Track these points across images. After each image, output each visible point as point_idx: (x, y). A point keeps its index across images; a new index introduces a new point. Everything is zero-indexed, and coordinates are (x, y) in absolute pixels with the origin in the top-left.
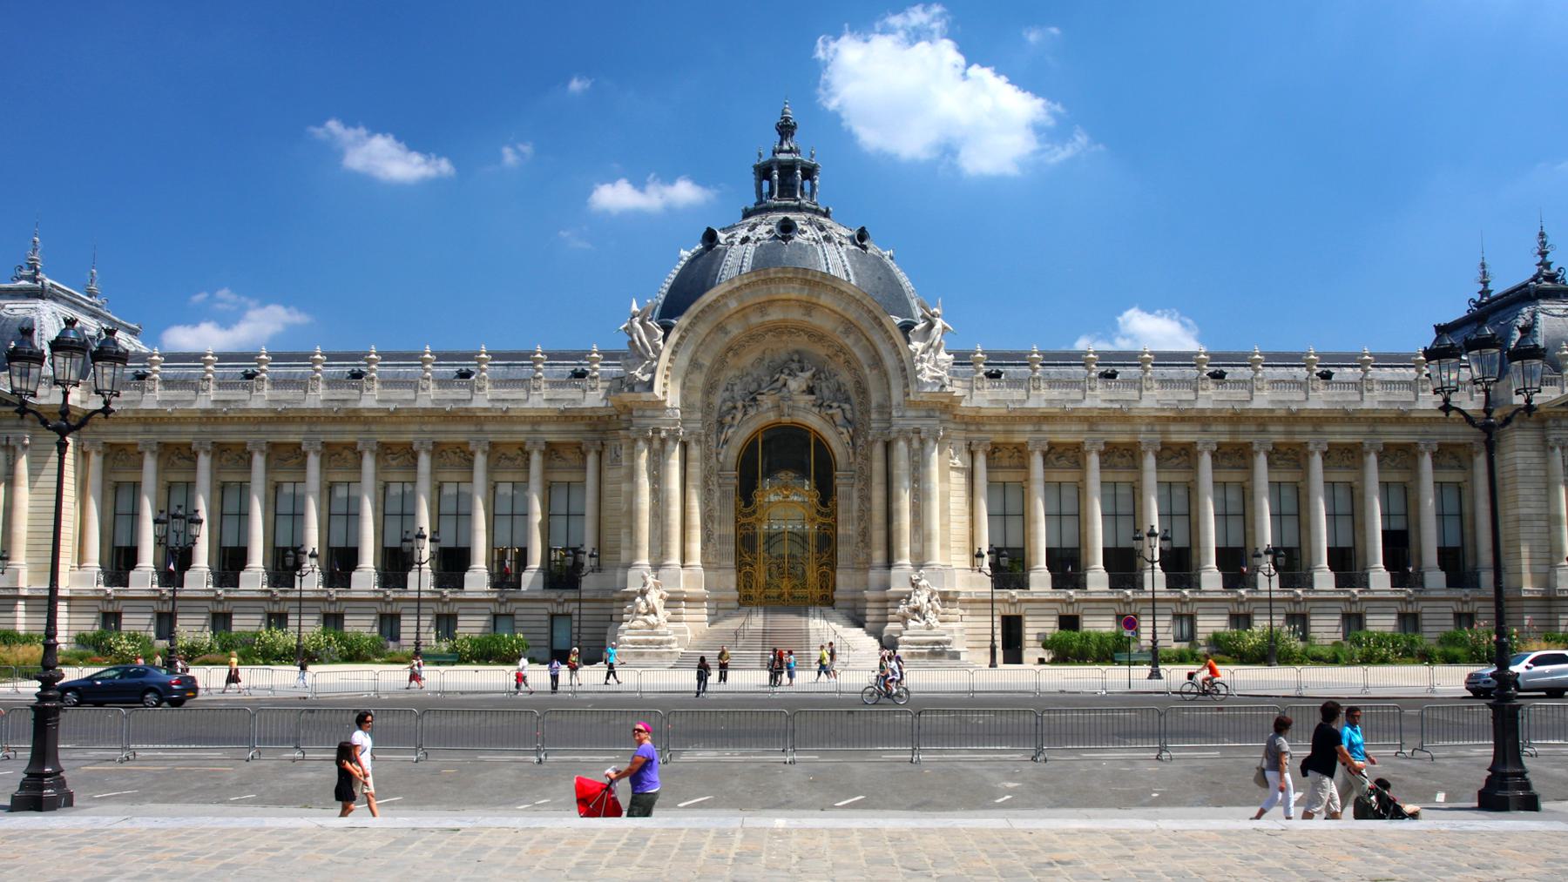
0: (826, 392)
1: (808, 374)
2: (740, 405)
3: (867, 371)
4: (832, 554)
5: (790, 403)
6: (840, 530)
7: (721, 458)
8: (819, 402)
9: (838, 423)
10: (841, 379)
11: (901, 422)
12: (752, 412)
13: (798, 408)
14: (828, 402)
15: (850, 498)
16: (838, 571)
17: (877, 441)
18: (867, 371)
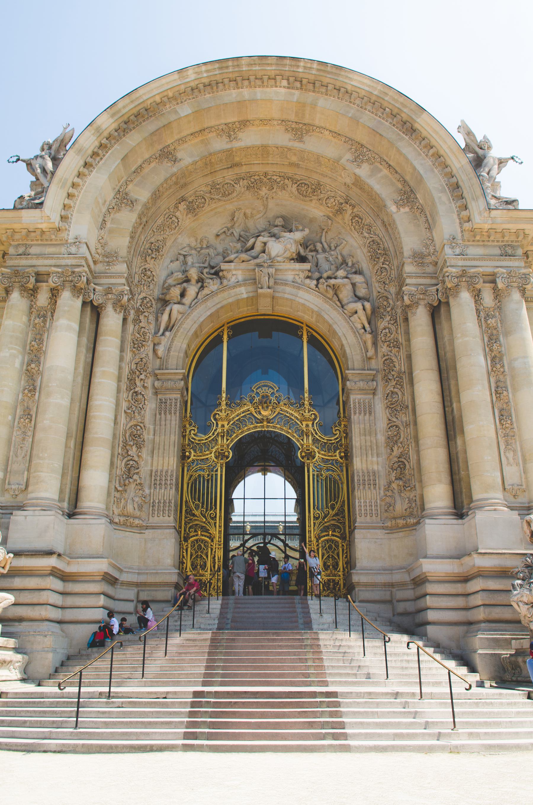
0: (324, 265)
1: (298, 236)
2: (193, 274)
3: (393, 208)
4: (341, 512)
5: (272, 271)
6: (358, 464)
7: (161, 350)
8: (317, 275)
9: (345, 301)
10: (345, 253)
11: (460, 263)
12: (213, 285)
13: (285, 283)
14: (329, 273)
15: (369, 410)
16: (358, 534)
17: (417, 304)
18: (393, 208)
